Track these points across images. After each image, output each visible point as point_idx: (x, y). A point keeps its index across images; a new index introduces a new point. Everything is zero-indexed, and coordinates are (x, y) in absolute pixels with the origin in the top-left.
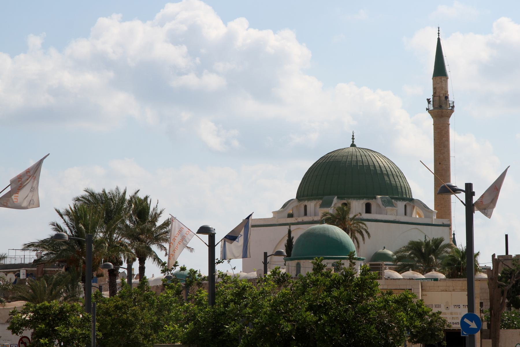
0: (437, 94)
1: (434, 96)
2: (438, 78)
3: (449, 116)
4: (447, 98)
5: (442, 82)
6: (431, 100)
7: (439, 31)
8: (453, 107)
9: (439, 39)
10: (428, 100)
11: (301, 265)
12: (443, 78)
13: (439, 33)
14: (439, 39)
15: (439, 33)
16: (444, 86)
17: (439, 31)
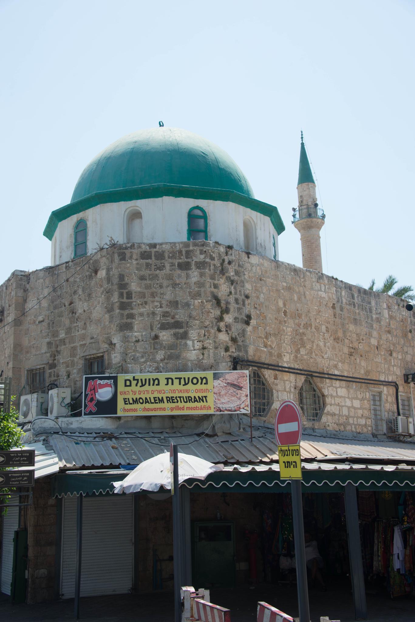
0: (305, 203)
1: (301, 202)
2: (305, 185)
3: (320, 228)
4: (316, 205)
5: (309, 189)
6: (298, 209)
7: (302, 135)
8: (324, 216)
9: (303, 144)
10: (294, 210)
11: (89, 224)
12: (311, 185)
13: (302, 138)
14: (303, 144)
15: (302, 138)
16: (312, 193)
17: (302, 135)
